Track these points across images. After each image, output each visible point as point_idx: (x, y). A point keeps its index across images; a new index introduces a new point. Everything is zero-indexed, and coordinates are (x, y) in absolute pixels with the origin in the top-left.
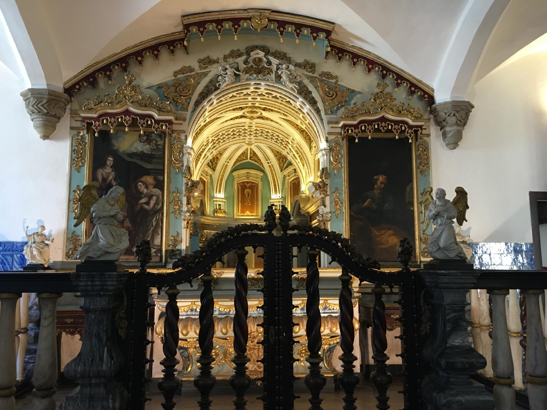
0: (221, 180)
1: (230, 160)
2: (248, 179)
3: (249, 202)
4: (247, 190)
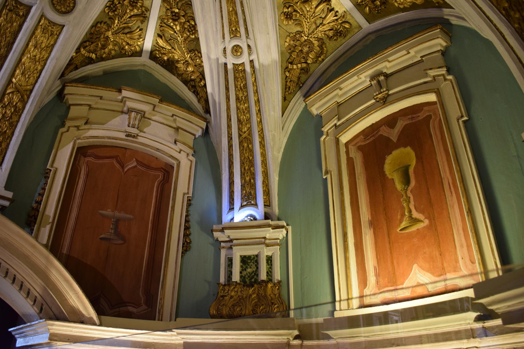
2: (385, 101)
3: (415, 214)
4: (396, 153)
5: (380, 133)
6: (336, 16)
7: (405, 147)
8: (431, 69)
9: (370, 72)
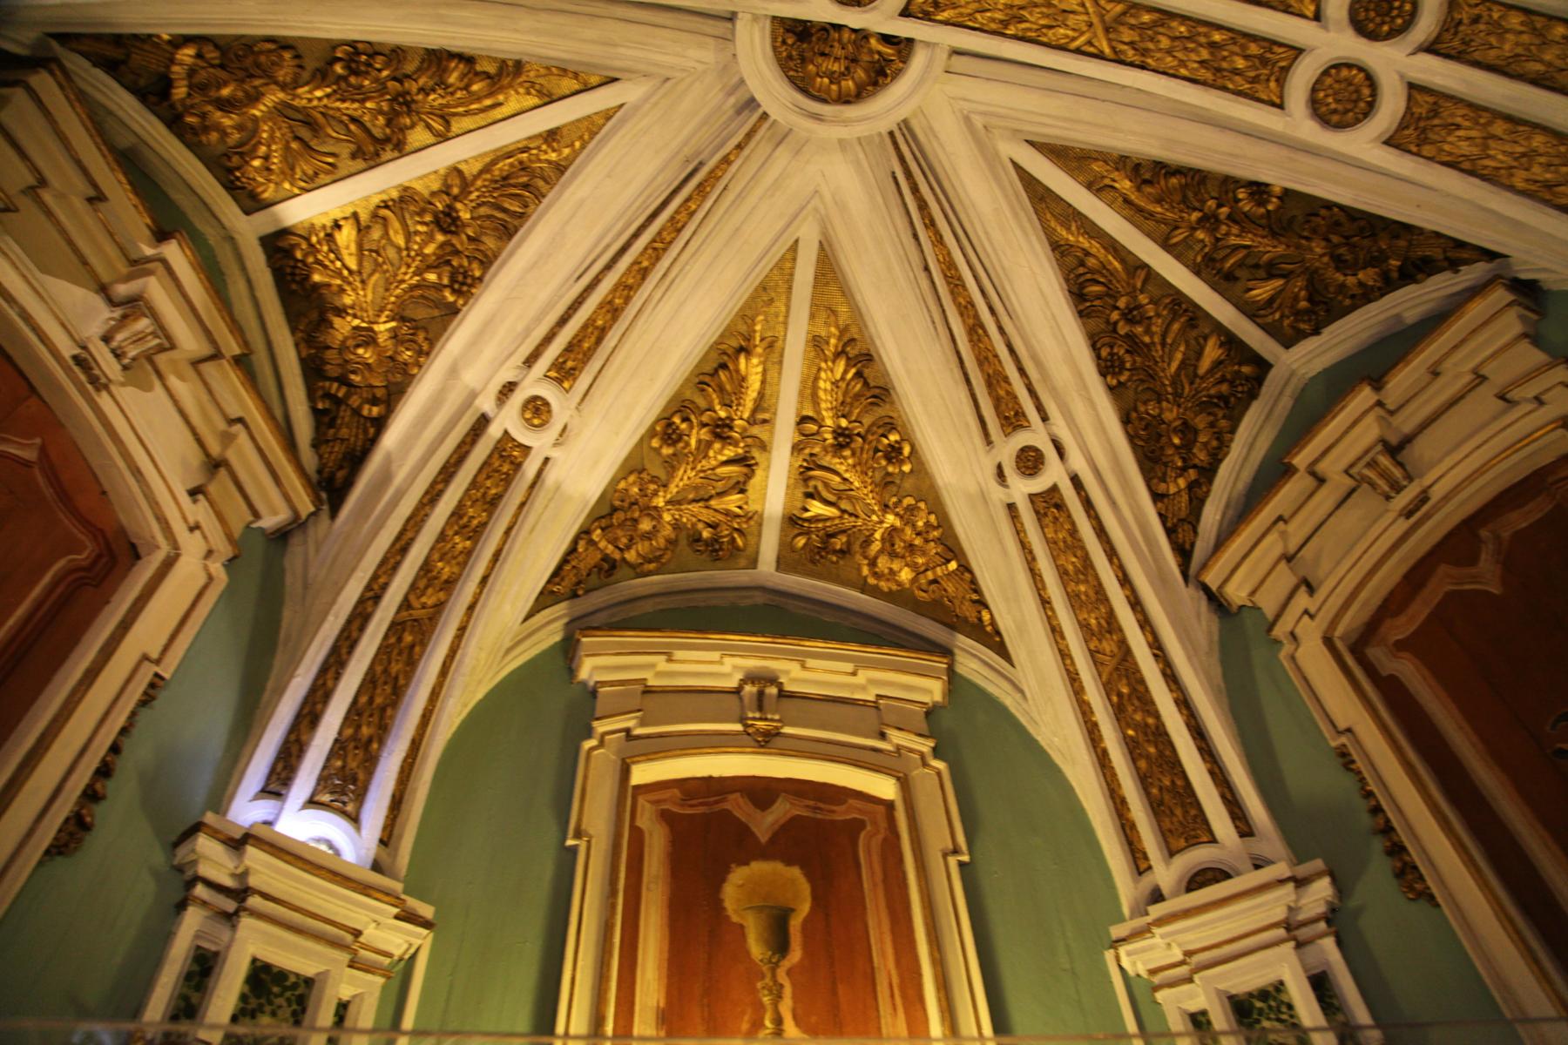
0: (396, 627)
1: (564, 373)
2: (766, 741)
4: (758, 867)
5: (727, 806)
6: (740, 507)
7: (789, 862)
8: (900, 729)
9: (753, 663)
